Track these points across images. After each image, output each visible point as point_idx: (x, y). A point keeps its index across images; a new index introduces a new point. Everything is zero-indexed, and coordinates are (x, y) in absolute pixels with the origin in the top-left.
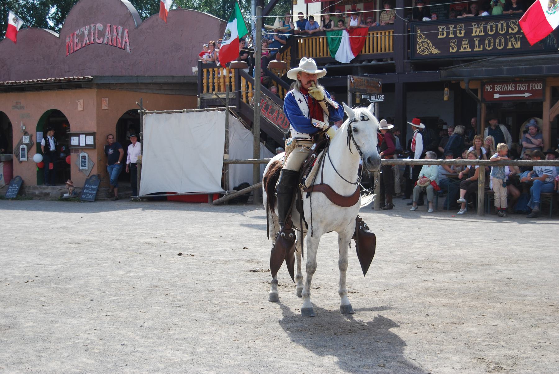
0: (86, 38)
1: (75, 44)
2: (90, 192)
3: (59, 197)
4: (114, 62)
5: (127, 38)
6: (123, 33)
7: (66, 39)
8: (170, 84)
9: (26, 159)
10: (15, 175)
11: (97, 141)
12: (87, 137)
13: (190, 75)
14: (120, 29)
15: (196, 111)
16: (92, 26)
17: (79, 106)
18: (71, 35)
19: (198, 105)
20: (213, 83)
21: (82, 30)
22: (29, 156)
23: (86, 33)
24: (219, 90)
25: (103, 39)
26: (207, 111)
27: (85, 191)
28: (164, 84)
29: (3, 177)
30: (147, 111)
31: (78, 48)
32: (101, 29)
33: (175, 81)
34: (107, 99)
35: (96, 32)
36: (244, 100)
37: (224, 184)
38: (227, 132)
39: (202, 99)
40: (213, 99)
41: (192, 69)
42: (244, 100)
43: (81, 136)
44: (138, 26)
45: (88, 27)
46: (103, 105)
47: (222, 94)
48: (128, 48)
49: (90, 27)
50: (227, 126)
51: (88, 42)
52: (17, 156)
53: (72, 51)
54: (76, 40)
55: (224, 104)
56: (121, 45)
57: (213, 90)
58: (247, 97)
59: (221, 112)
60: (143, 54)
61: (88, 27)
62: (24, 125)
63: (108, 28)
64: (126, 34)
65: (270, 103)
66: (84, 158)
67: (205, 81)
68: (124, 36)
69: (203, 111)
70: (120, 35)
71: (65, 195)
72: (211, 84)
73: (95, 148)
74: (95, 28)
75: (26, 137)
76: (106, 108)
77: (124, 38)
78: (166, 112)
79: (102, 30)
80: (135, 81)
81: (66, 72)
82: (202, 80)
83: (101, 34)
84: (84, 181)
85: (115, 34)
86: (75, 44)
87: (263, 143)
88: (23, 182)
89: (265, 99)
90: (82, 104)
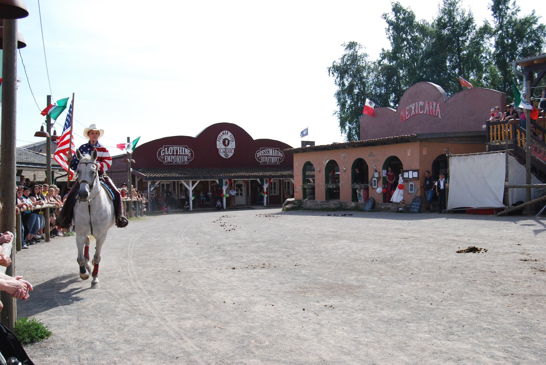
0: (413, 111)
1: (406, 115)
2: (415, 207)
3: (396, 210)
4: (431, 125)
5: (439, 109)
6: (436, 106)
7: (400, 113)
8: (467, 137)
9: (376, 187)
10: (370, 197)
11: (419, 175)
12: (414, 172)
13: (481, 130)
14: (434, 104)
15: (485, 154)
16: (417, 103)
17: (408, 153)
18: (404, 110)
19: (487, 150)
20: (497, 135)
21: (410, 106)
22: (378, 185)
23: (413, 108)
24: (501, 139)
25: (424, 111)
26: (493, 153)
27: (412, 207)
28: (463, 137)
29: (363, 198)
30: (452, 155)
31: (408, 118)
32: (422, 105)
33: (471, 135)
34: (426, 148)
35: (419, 107)
36: (519, 145)
37: (505, 201)
38: (507, 167)
39: (489, 146)
40: (497, 145)
41: (482, 127)
42: (519, 145)
43: (410, 172)
44: (446, 101)
45: (414, 104)
46: (424, 152)
47: (504, 141)
48: (440, 116)
49: (416, 104)
50: (507, 162)
51: (414, 113)
52: (371, 185)
53: (404, 120)
54: (407, 113)
55: (504, 148)
56: (435, 114)
57: (497, 139)
58: (521, 143)
59: (502, 153)
60: (449, 119)
61: (414, 104)
62: (375, 166)
63: (427, 104)
64: (438, 107)
65: (538, 146)
66: (412, 185)
67: (491, 134)
68: (437, 108)
69: (490, 153)
70: (434, 108)
71: (400, 209)
72: (495, 136)
73: (418, 179)
74: (419, 105)
75: (376, 173)
76: (425, 154)
77: (437, 109)
78: (464, 155)
79: (422, 105)
80: (444, 136)
81: (401, 133)
82: (489, 132)
83: (422, 108)
84: (412, 200)
85: (431, 107)
86: (406, 115)
87: (533, 174)
88: (375, 201)
89: (534, 144)
90: (410, 152)
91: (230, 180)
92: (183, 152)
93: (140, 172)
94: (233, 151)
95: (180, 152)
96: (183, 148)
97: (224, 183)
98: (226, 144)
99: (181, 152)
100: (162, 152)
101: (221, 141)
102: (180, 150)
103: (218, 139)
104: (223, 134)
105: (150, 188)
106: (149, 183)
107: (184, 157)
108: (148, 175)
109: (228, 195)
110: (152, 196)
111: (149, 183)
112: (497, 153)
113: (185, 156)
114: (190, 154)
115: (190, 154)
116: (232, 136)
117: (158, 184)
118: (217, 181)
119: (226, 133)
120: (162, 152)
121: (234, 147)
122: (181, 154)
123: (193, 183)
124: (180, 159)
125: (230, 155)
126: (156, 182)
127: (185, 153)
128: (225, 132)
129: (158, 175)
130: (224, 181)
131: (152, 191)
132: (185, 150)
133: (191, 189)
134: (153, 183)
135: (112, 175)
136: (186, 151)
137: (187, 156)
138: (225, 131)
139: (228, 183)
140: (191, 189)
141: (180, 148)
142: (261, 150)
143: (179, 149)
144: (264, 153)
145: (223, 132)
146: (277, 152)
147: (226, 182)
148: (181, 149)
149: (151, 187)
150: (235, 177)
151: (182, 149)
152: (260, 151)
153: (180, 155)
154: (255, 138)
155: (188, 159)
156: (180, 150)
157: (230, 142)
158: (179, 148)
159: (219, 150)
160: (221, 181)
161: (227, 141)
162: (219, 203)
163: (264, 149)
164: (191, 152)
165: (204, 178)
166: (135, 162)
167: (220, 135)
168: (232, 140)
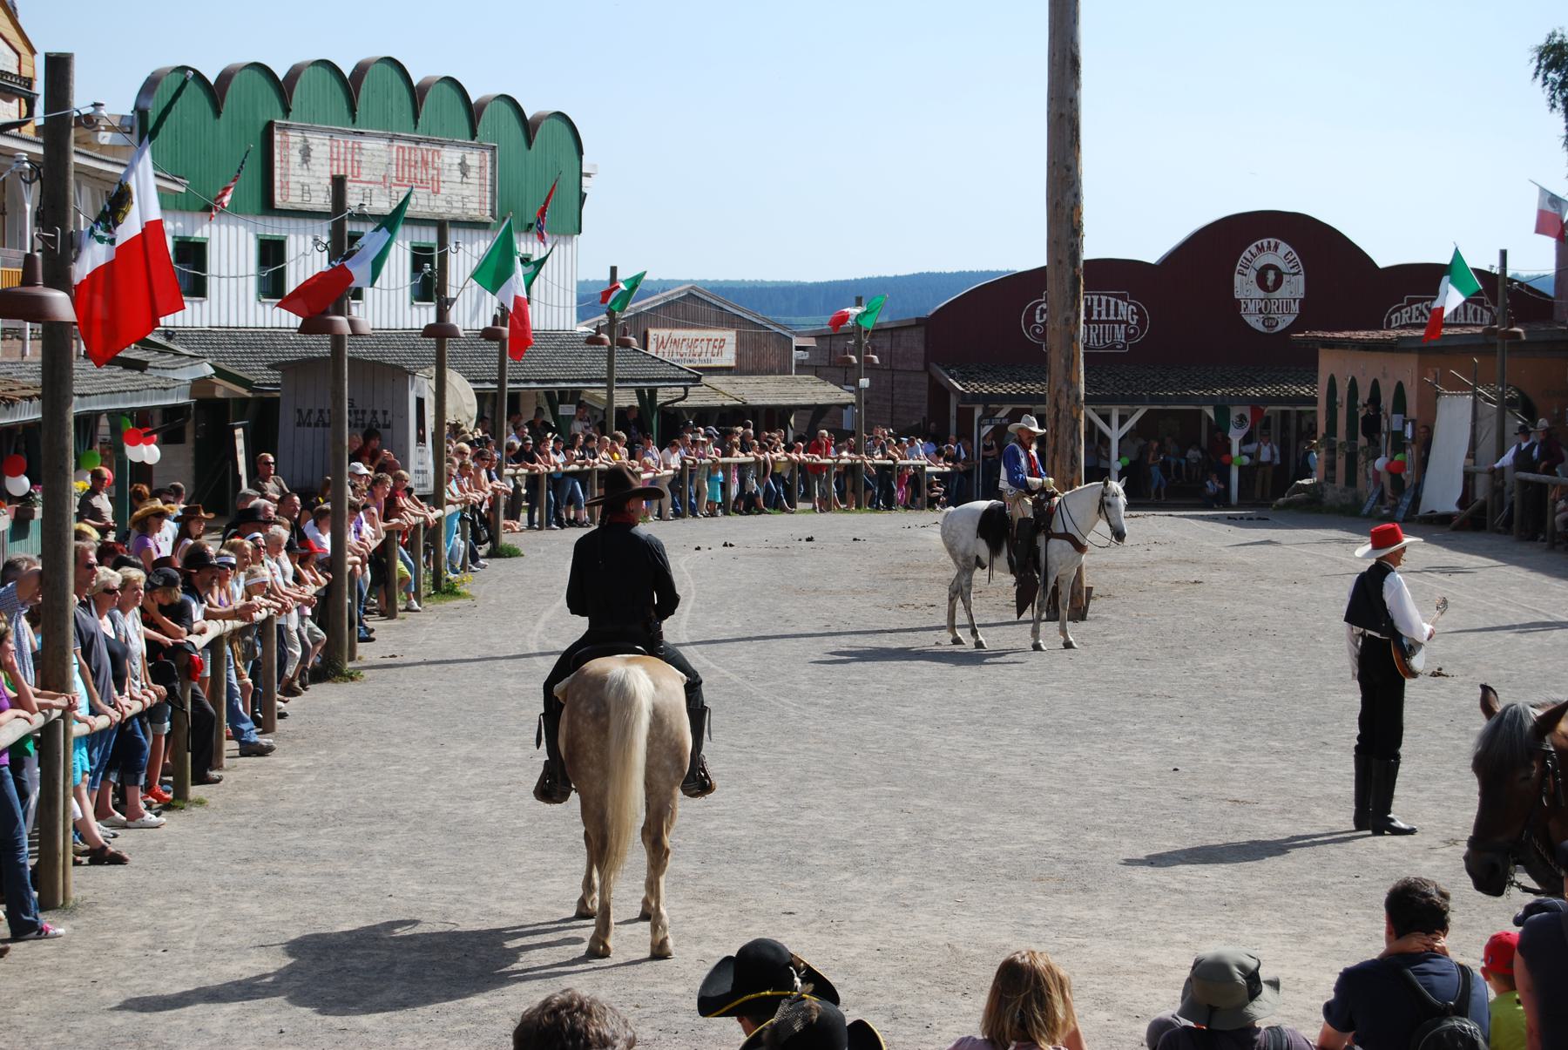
91: (1256, 412)
92: (1112, 312)
93: (951, 377)
94: (1295, 308)
95: (1099, 314)
96: (1112, 300)
97: (1233, 418)
98: (1270, 283)
99: (1104, 313)
100: (1038, 312)
101: (1253, 275)
102: (1100, 305)
103: (1238, 267)
104: (1260, 249)
105: (980, 426)
106: (978, 412)
107: (1113, 327)
108: (974, 387)
109: (1246, 460)
110: (987, 453)
111: (978, 412)
112: (1462, 395)
113: (1117, 326)
114: (1136, 317)
115: (1136, 317)
116: (1295, 255)
117: (1006, 417)
118: (1210, 411)
119: (1269, 247)
120: (1038, 312)
121: (1300, 292)
122: (1104, 317)
123: (1123, 420)
124: (1098, 335)
125: (1285, 321)
126: (999, 410)
127: (1116, 315)
128: (1265, 245)
129: (1002, 389)
130: (1235, 412)
131: (985, 438)
132: (1116, 304)
133: (1115, 434)
134: (989, 415)
135: (895, 378)
136: (1121, 307)
137: (1123, 326)
138: (1265, 241)
139: (1249, 419)
140: (1115, 434)
141: (1100, 300)
142: (1411, 302)
143: (1095, 303)
144: (1422, 314)
145: (1259, 243)
146: (1475, 311)
147: (1242, 418)
148: (1104, 303)
149: (984, 426)
150: (1268, 400)
151: (1108, 302)
152: (1405, 307)
153: (1099, 322)
154: (1382, 261)
155: (1128, 336)
156: (1100, 305)
157: (1286, 278)
158: (1096, 298)
159: (1243, 306)
160: (1222, 411)
161: (1271, 276)
162: (1212, 486)
163: (1422, 301)
164: (1140, 313)
165: (1154, 400)
166: (877, 361)
167: (1246, 254)
168: (1296, 271)
